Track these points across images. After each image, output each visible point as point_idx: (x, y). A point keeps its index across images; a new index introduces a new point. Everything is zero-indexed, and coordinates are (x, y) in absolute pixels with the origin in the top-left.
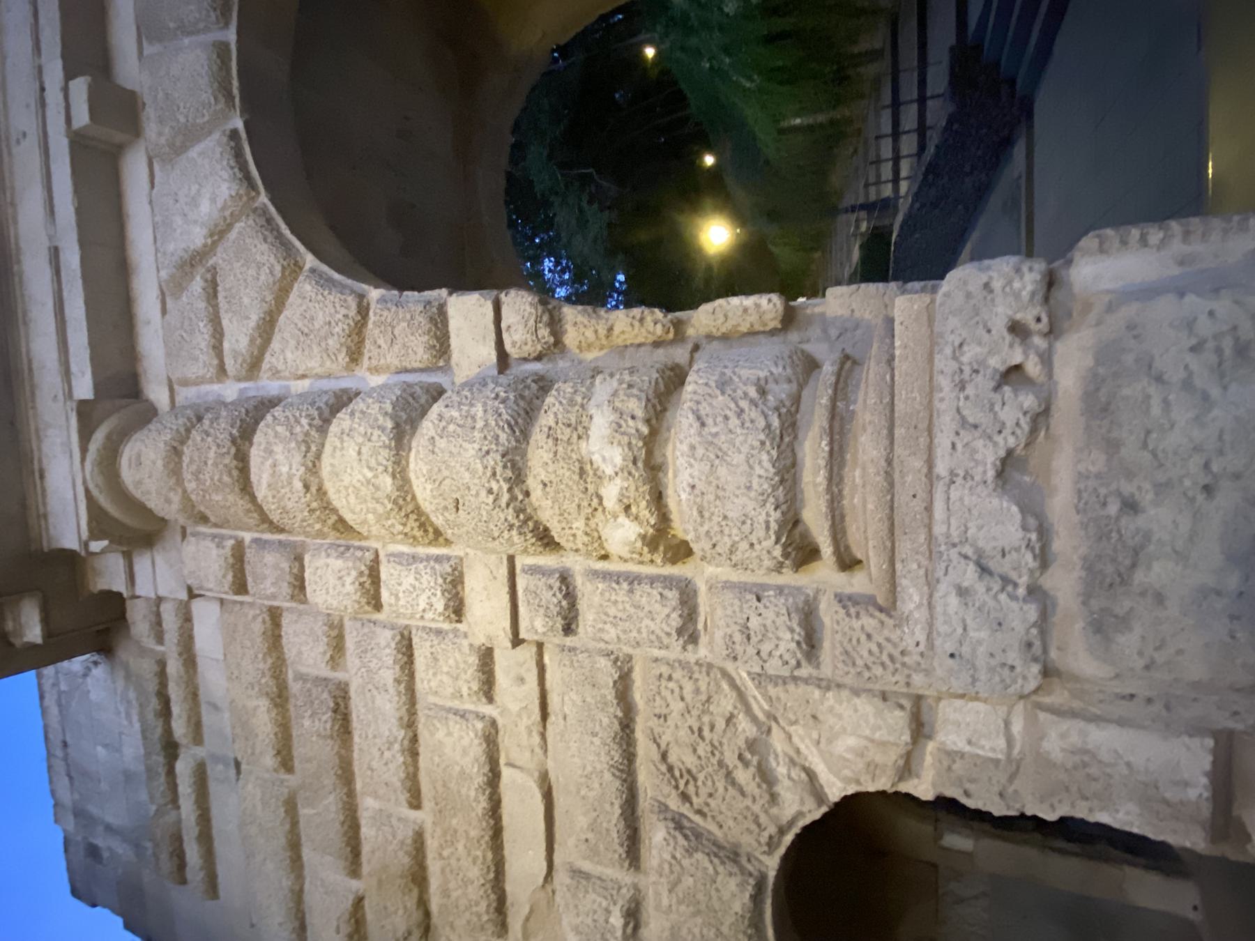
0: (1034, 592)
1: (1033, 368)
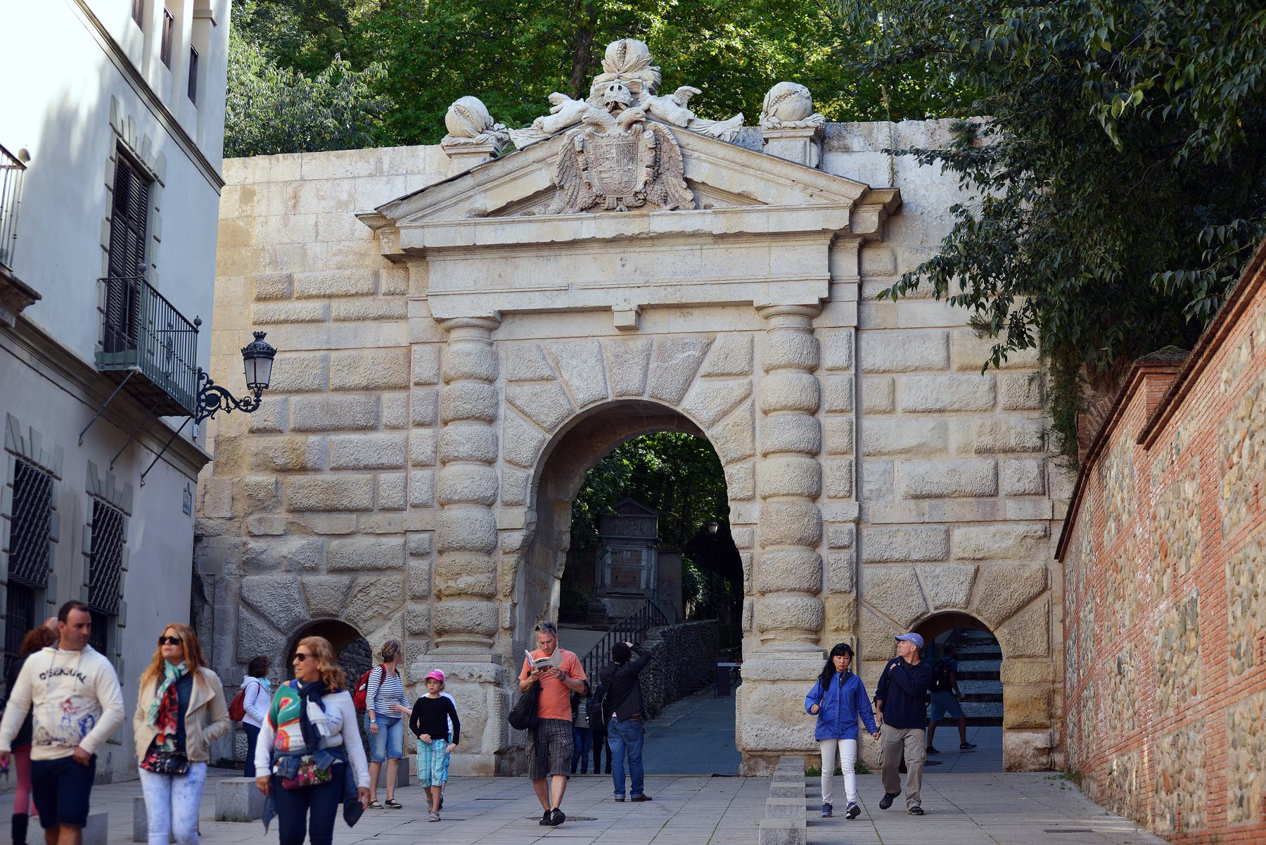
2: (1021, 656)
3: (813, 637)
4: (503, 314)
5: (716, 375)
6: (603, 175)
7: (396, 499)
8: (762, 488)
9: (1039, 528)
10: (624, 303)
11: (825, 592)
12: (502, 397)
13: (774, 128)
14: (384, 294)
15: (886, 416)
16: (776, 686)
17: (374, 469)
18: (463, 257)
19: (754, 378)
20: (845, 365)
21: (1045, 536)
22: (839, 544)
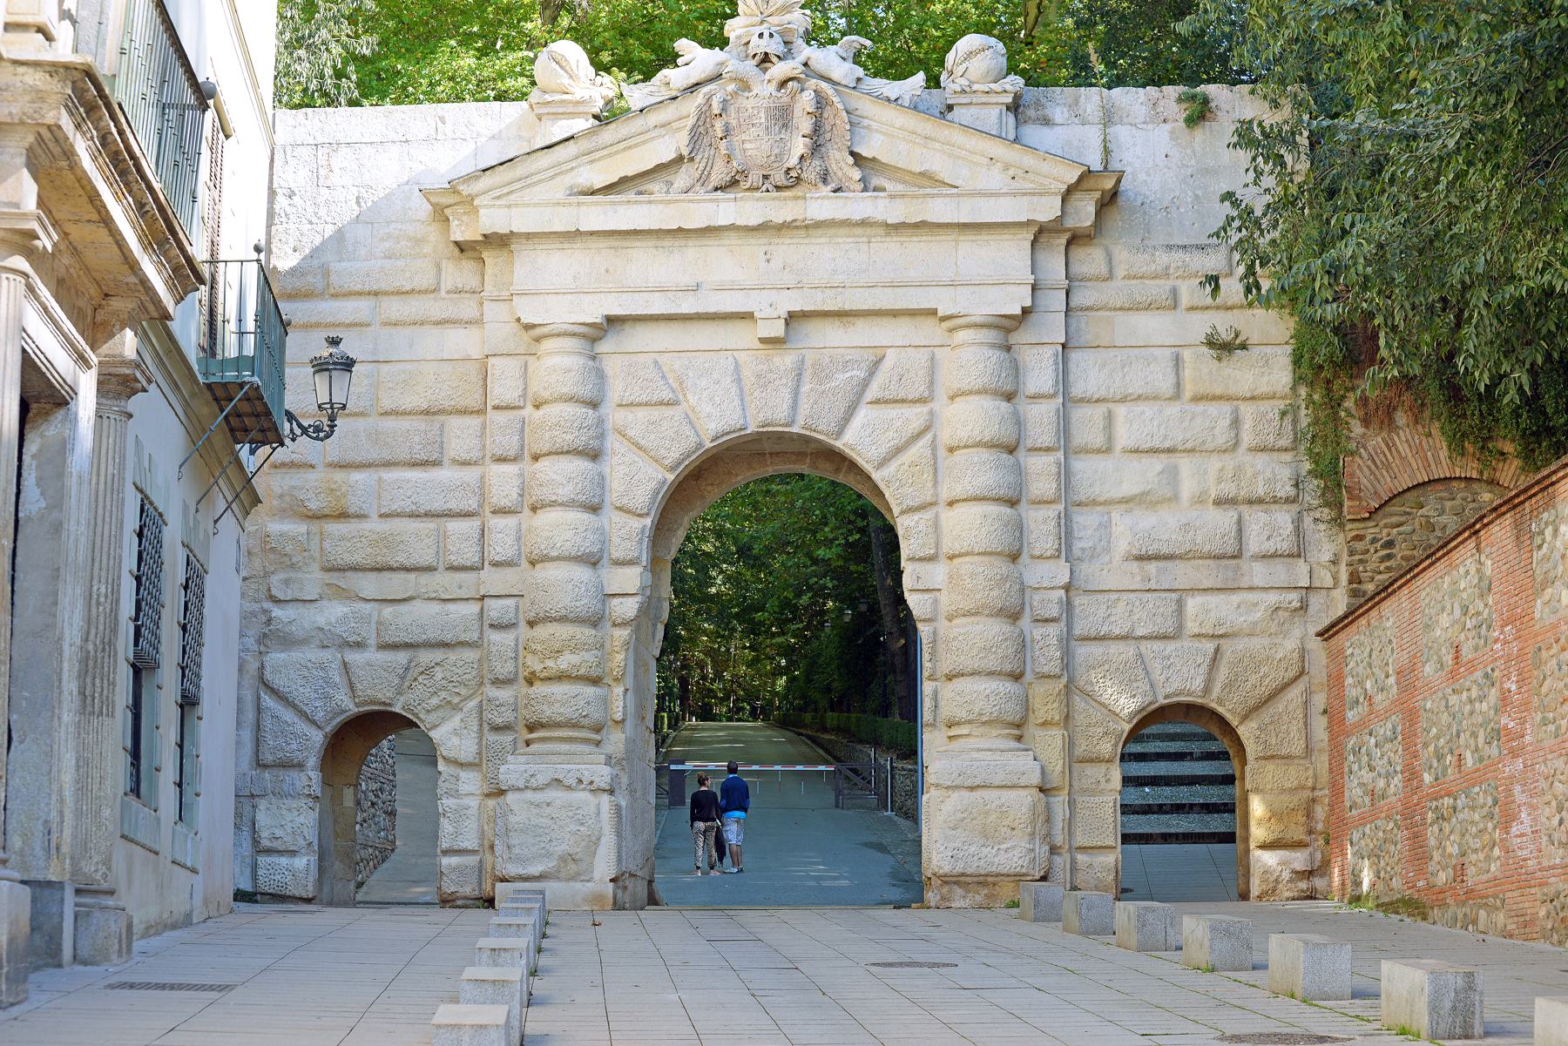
0: (527, 787)
1: (582, 786)
2: (1273, 757)
3: (1016, 732)
4: (612, 321)
5: (886, 402)
6: (747, 146)
7: (470, 556)
8: (948, 545)
9: (1294, 598)
10: (771, 308)
11: (1029, 677)
12: (609, 425)
13: (964, 91)
14: (448, 292)
15: (1100, 456)
16: (975, 794)
17: (438, 516)
18: (560, 246)
19: (935, 405)
20: (1051, 391)
21: (1301, 608)
22: (1047, 616)
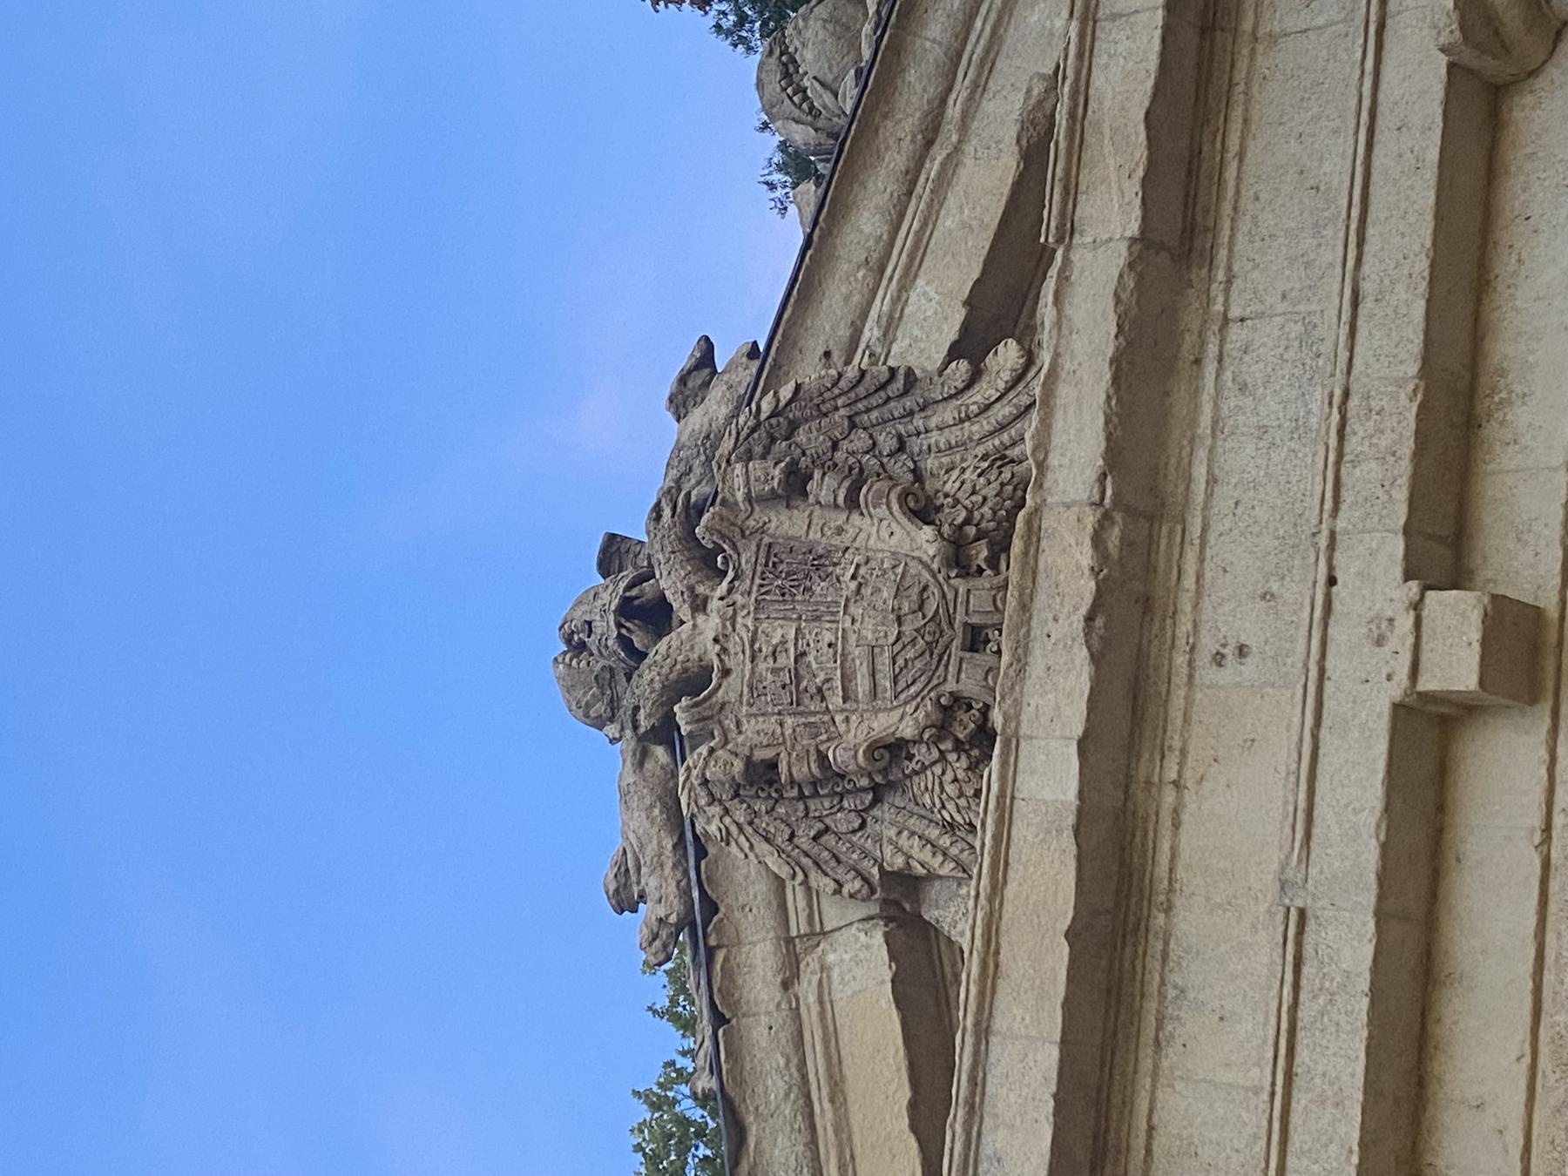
6: (862, 686)
